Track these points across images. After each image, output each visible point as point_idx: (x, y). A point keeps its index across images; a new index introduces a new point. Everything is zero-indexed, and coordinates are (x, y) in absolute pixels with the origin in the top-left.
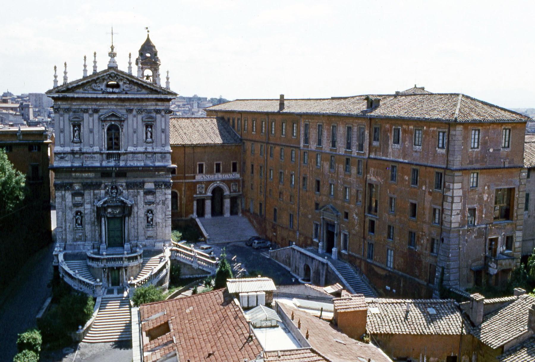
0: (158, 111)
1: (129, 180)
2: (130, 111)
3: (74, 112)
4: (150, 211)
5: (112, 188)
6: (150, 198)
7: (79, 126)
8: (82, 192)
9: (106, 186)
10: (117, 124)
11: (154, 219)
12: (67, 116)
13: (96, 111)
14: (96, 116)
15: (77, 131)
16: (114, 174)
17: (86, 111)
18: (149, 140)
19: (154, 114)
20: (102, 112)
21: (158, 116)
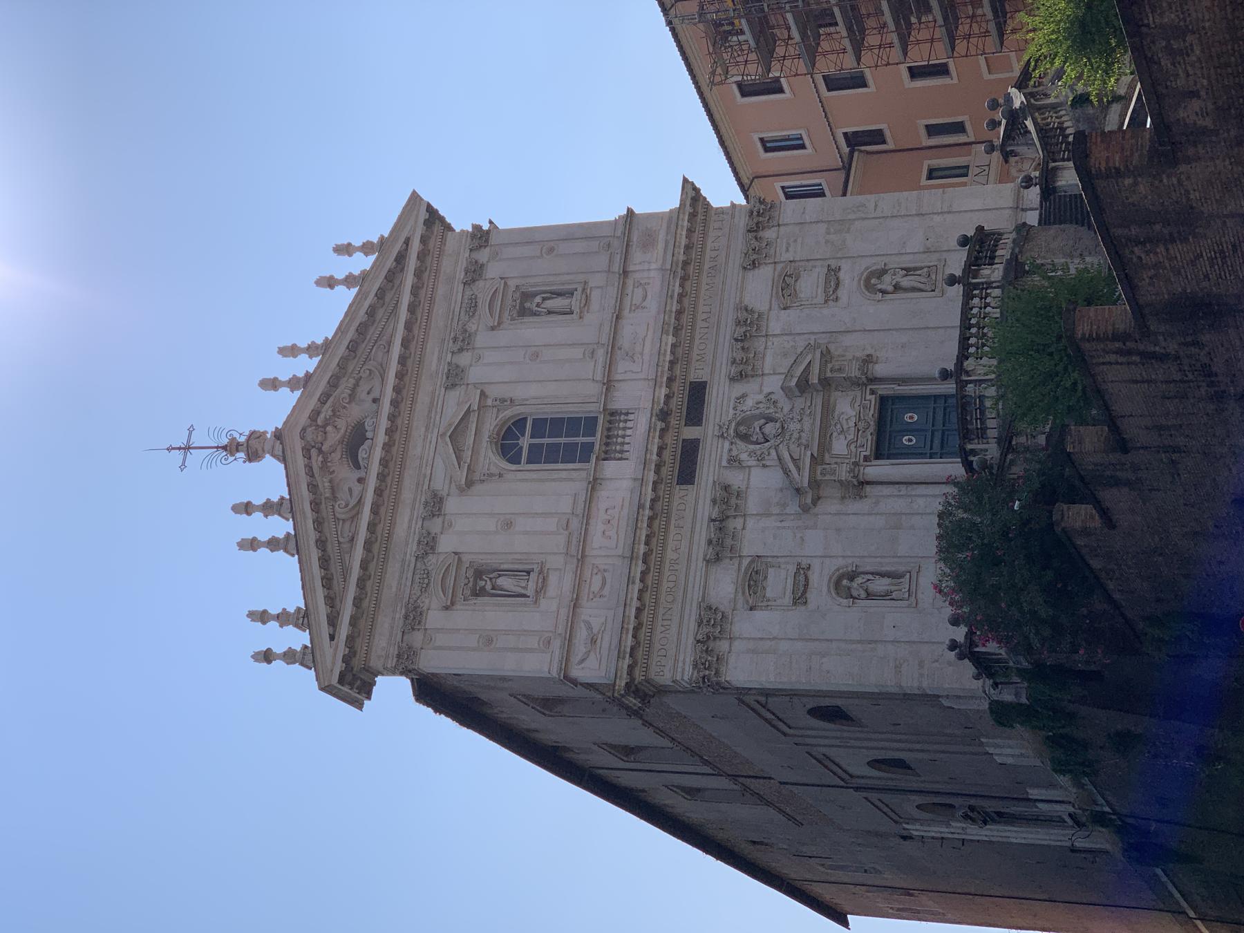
0: (475, 272)
1: (724, 369)
2: (454, 377)
3: (425, 589)
4: (873, 282)
5: (745, 438)
6: (810, 285)
7: (479, 574)
8: (745, 562)
9: (734, 461)
10: (491, 424)
11: (907, 261)
12: (435, 618)
13: (435, 505)
14: (453, 505)
15: (501, 581)
16: (690, 433)
17: (428, 544)
18: (575, 302)
19: (483, 290)
20: (439, 484)
21: (493, 271)
